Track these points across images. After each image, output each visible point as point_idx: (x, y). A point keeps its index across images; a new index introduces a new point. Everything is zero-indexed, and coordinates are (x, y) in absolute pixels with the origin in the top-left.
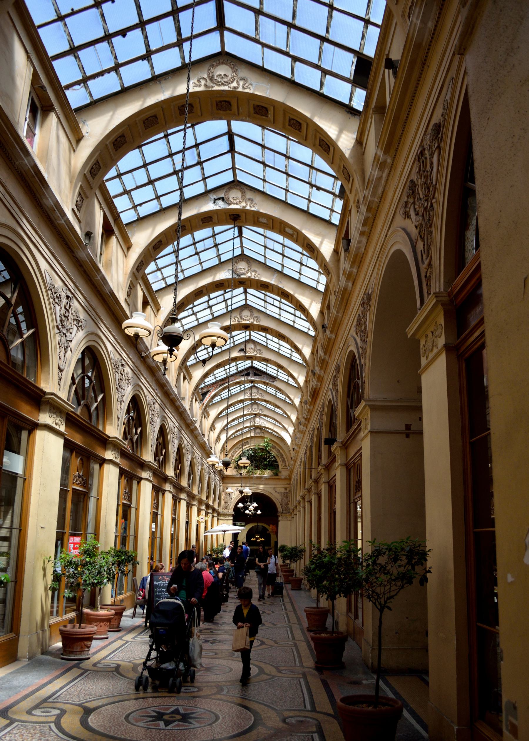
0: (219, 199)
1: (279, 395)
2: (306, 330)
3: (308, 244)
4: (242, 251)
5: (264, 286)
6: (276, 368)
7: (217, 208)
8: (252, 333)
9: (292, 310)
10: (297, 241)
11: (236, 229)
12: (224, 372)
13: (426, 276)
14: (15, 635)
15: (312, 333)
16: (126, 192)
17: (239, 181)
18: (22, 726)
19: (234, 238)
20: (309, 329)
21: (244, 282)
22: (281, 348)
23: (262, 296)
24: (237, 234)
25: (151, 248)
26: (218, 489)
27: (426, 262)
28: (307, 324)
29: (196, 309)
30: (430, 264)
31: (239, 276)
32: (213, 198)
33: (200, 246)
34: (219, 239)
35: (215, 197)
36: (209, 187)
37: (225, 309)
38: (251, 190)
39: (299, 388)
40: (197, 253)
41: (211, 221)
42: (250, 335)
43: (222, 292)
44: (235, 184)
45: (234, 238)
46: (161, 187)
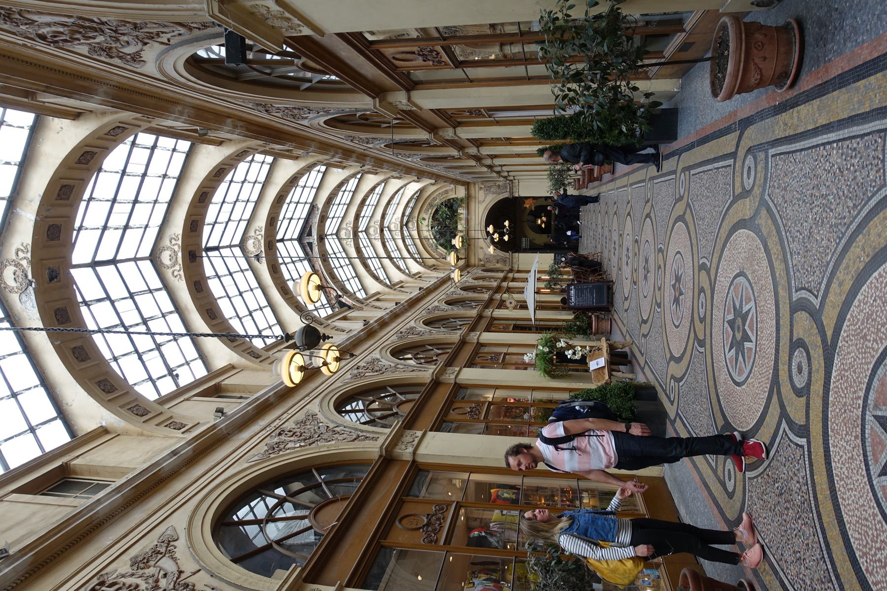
3: (79, 162)
4: (235, 246)
5: (272, 221)
6: (365, 208)
8: (279, 237)
10: (83, 180)
11: (210, 254)
12: (345, 268)
15: (323, 168)
17: (151, 255)
19: (222, 256)
20: (319, 171)
24: (216, 253)
26: (480, 273)
28: (314, 173)
29: (243, 312)
37: (246, 273)
39: (386, 181)
41: (199, 282)
42: (332, 235)
45: (222, 256)
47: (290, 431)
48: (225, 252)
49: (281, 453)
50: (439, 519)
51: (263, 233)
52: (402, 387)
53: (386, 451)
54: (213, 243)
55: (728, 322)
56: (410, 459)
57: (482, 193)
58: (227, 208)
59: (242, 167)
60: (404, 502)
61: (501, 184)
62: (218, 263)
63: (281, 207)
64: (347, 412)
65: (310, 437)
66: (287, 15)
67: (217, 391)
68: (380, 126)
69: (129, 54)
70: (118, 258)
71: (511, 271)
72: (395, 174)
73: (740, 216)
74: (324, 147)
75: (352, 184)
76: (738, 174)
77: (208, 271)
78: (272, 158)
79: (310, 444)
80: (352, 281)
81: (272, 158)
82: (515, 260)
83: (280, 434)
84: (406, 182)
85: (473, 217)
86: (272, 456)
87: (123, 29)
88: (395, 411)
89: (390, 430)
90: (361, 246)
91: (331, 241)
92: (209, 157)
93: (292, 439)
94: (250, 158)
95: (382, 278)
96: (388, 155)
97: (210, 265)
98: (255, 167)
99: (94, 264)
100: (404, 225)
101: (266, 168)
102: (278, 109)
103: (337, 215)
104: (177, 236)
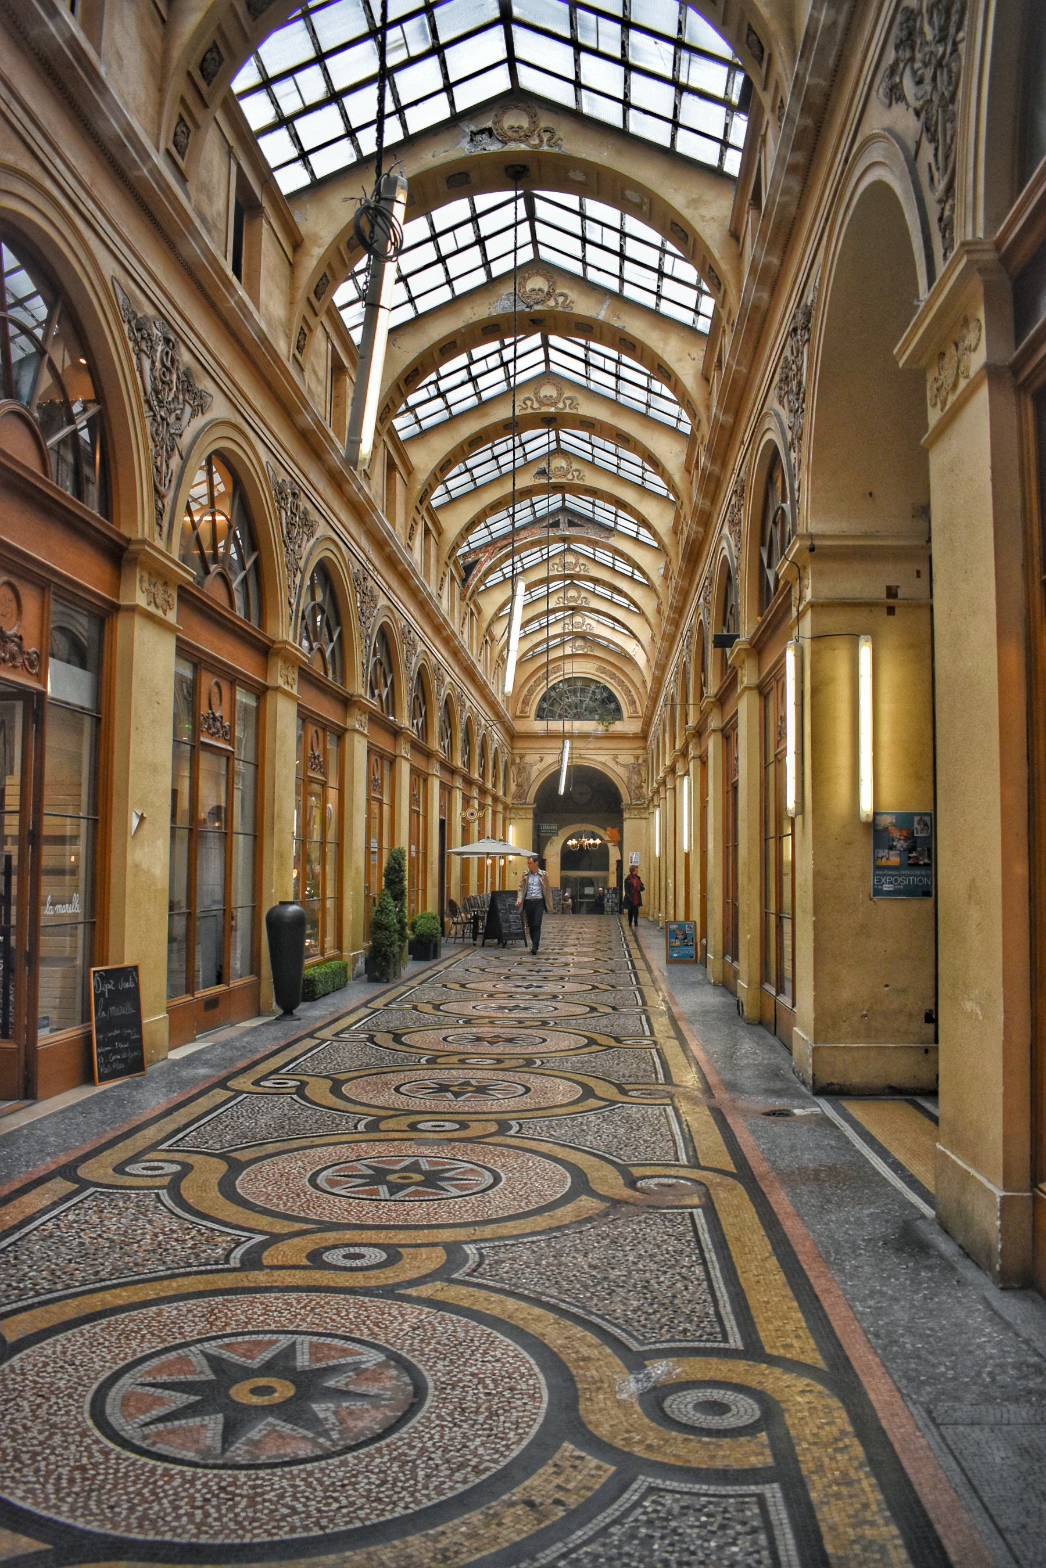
0: (482, 132)
2: (673, 422)
4: (536, 251)
6: (613, 509)
7: (477, 151)
9: (643, 380)
11: (521, 202)
13: (940, 219)
15: (686, 429)
16: (284, 122)
18: (102, 1193)
19: (517, 223)
23: (580, 352)
24: (522, 214)
27: (941, 186)
28: (674, 409)
30: (950, 188)
32: (467, 131)
33: (447, 244)
34: (487, 225)
35: (473, 128)
39: (661, 550)
40: (441, 260)
43: (495, 345)
45: (517, 223)
47: (173, 361)
48: (540, 355)
49: (131, 344)
50: (13, 657)
51: (576, 481)
52: (260, 578)
53: (138, 552)
54: (542, 209)
55: (417, 1163)
56: (124, 602)
57: (631, 760)
58: (612, 240)
59: (688, 272)
60: (43, 589)
61: (644, 790)
62: (505, 216)
63: (612, 346)
64: (210, 474)
65: (160, 402)
66: (963, 384)
67: (246, 209)
68: (763, 544)
69: (901, 81)
70: (515, 28)
71: (506, 808)
72: (666, 610)
73: (591, 1174)
74: (723, 442)
75: (656, 483)
76: (660, 1170)
77: (484, 201)
78: (707, 331)
79: (148, 402)
80: (466, 477)
81: (707, 331)
82: (521, 813)
83: (167, 341)
84: (647, 649)
85: (591, 746)
86: (126, 327)
87: (943, 78)
88: (213, 567)
89: (175, 556)
90: (535, 499)
91: (544, 440)
92: (710, 214)
93: (158, 364)
94: (705, 287)
95: (471, 538)
96: (707, 567)
98: (689, 297)
100: (582, 636)
101: (686, 317)
102: (799, 352)
103: (597, 510)
104: (556, 144)
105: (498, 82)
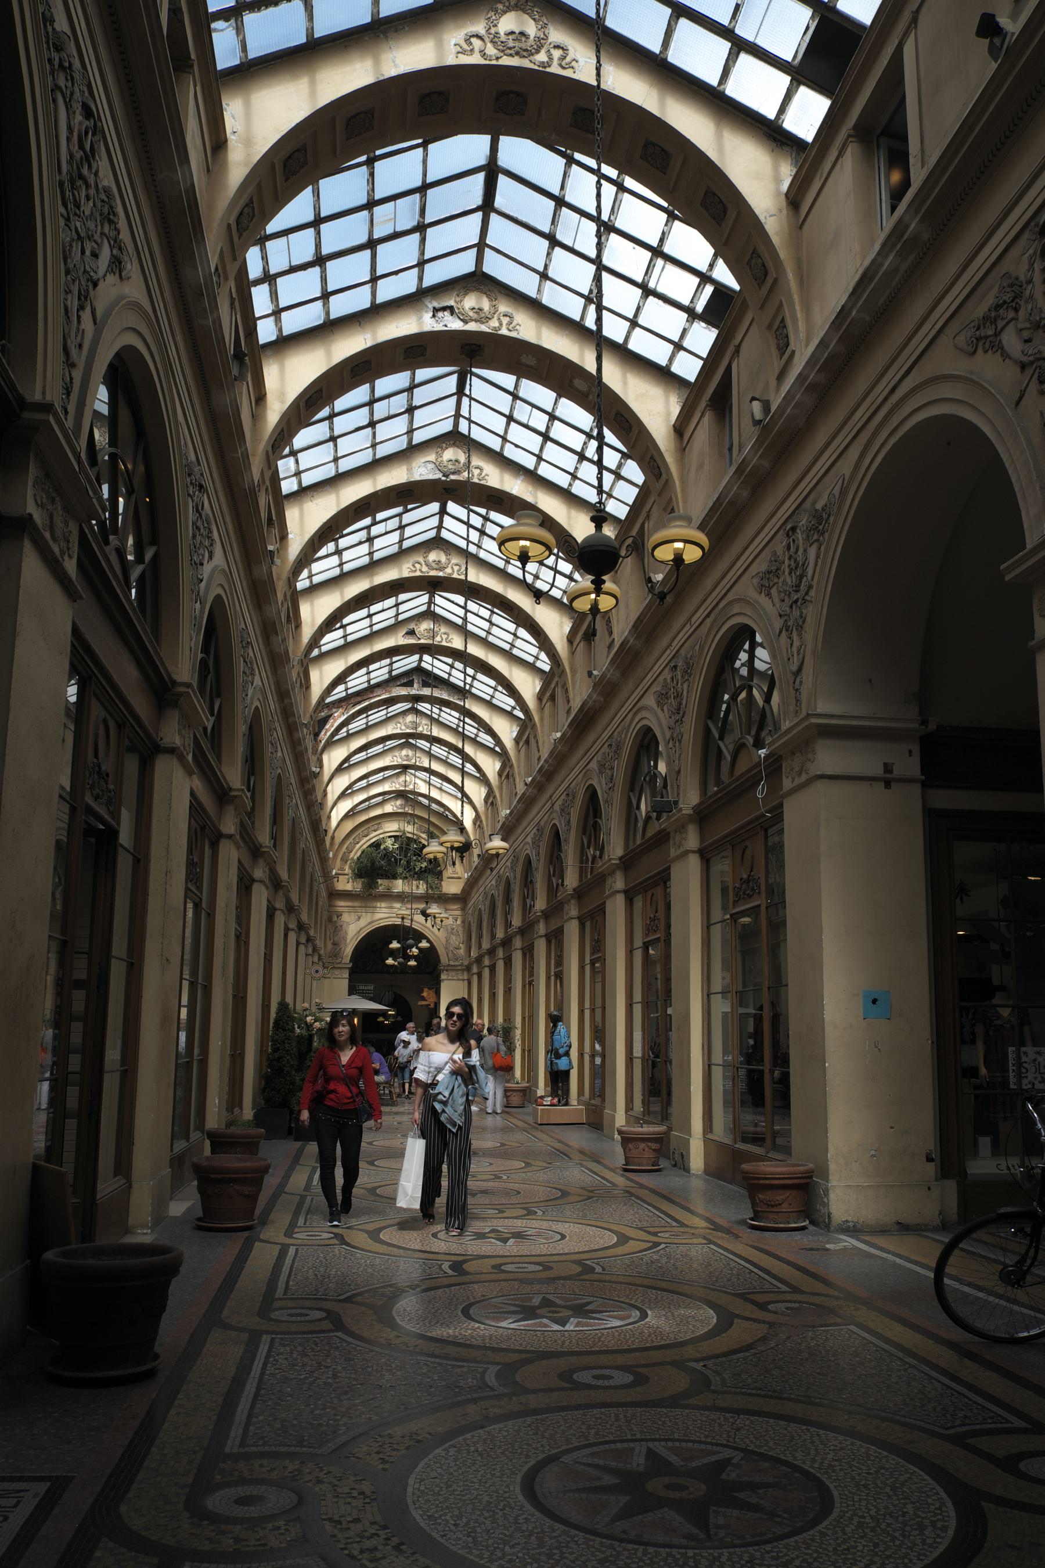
0: (444, 309)
1: (471, 730)
14: (124, 1181)
21: (454, 490)
22: (495, 630)
25: (302, 404)
31: (447, 476)
32: (430, 306)
35: (436, 304)
36: (427, 283)
38: (508, 295)
44: (478, 280)
46: (339, 272)
97: (438, 382)
99: (492, 171)
105: (464, 264)
